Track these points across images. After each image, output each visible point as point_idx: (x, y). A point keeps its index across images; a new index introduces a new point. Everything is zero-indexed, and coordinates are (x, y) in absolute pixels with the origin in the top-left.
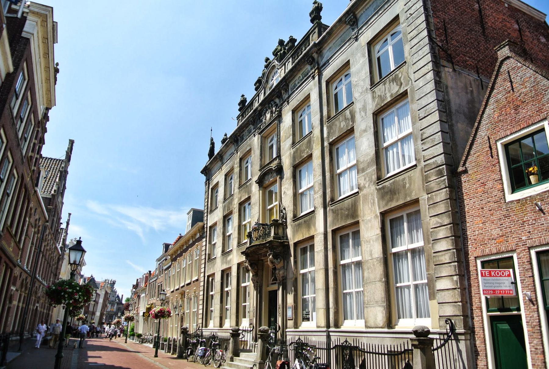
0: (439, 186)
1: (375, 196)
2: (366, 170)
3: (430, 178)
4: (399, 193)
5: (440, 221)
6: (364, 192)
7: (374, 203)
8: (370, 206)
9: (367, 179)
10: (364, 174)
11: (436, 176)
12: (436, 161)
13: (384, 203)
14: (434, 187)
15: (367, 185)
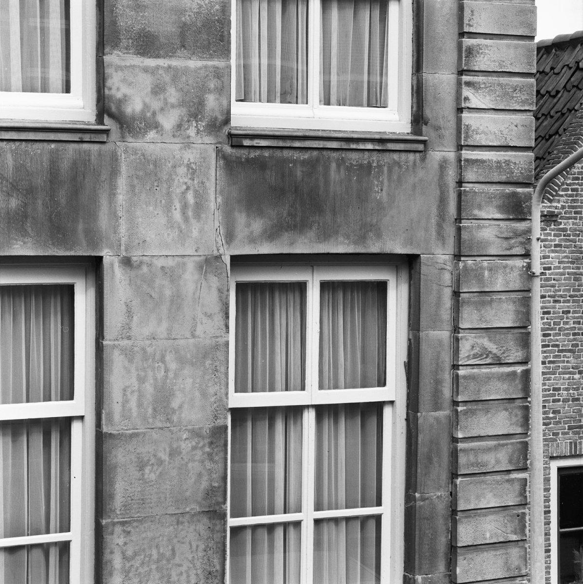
0: (505, 244)
1: (211, 186)
2: (170, 53)
3: (480, 207)
4: (334, 213)
5: (492, 347)
6: (149, 144)
7: (199, 207)
8: (177, 215)
9: (173, 95)
10: (151, 62)
11: (501, 208)
12: (508, 162)
13: (258, 226)
14: (488, 243)
15: (168, 121)
